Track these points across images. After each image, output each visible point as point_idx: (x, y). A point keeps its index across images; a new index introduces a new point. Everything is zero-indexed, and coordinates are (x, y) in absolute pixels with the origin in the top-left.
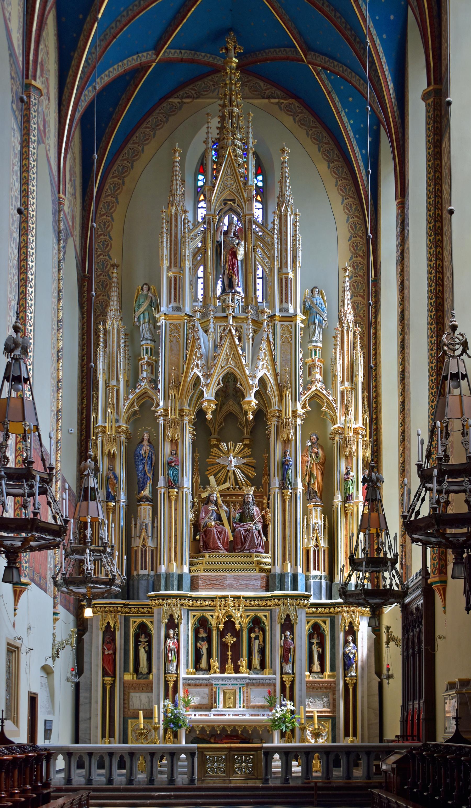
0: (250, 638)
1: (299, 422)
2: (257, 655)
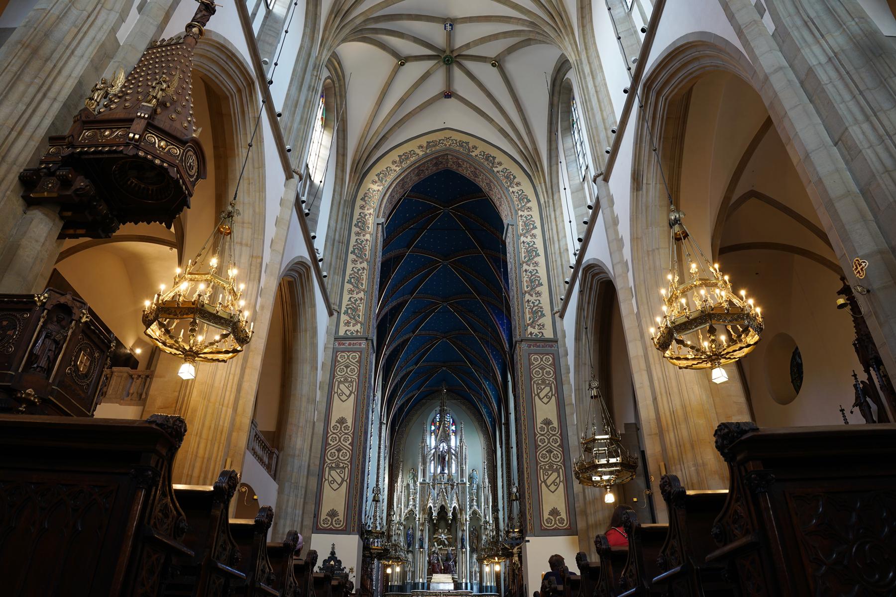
1: (468, 523)
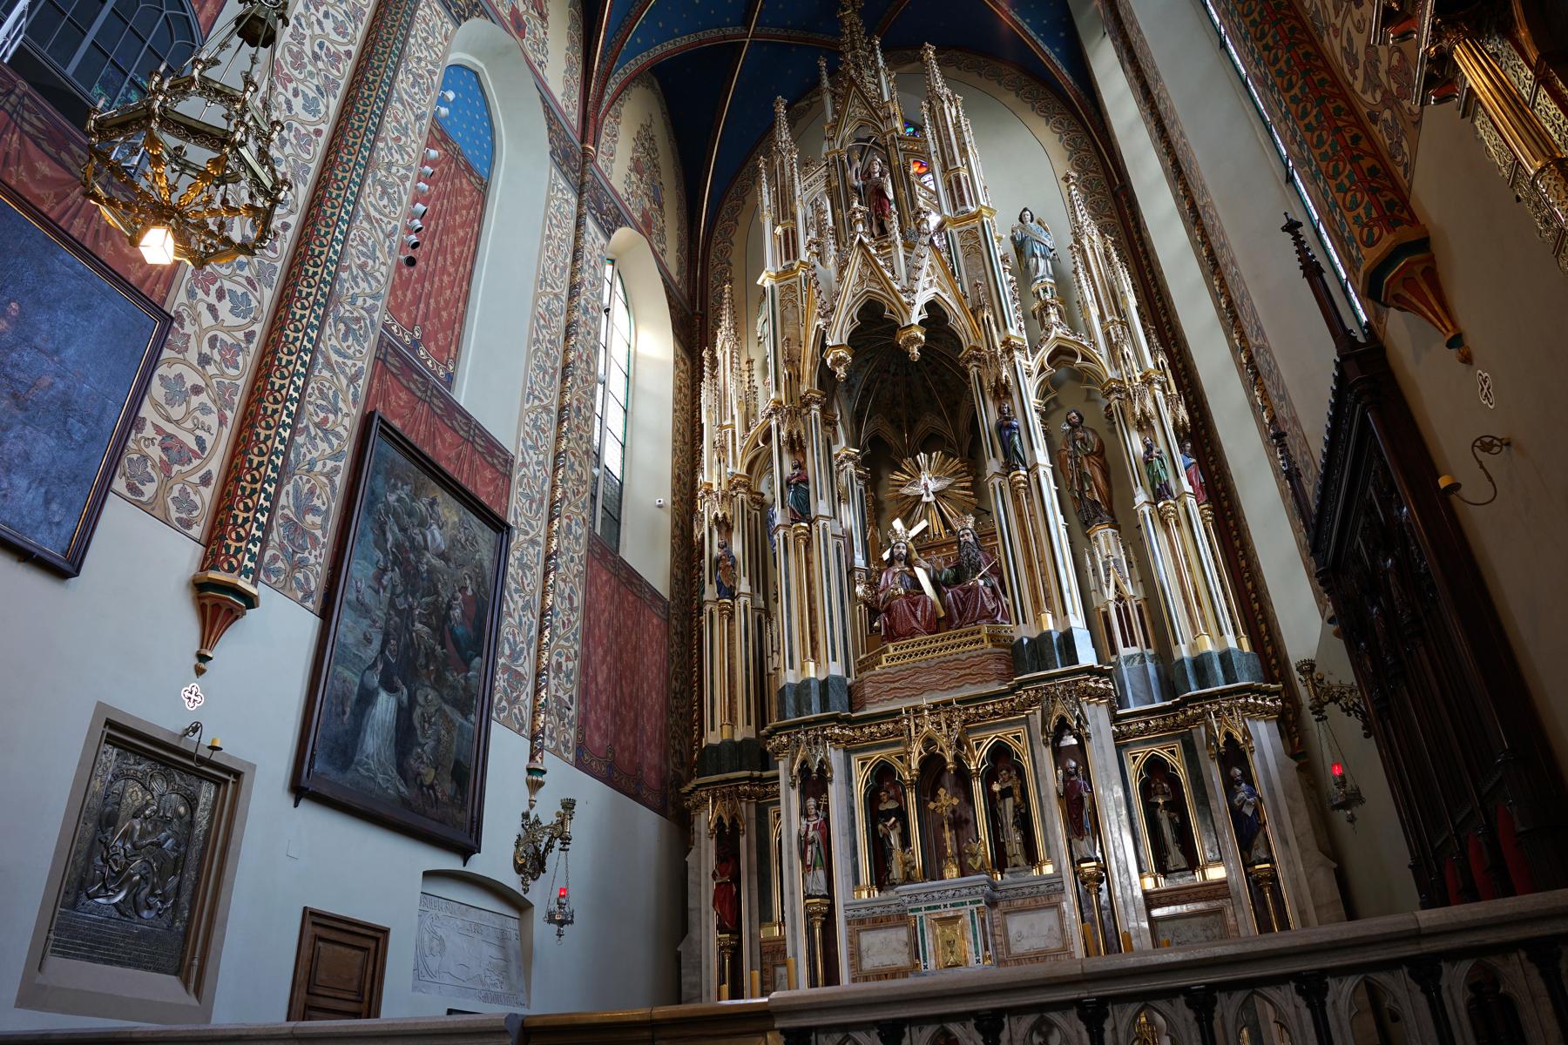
0: (990, 796)
2: (1012, 830)
